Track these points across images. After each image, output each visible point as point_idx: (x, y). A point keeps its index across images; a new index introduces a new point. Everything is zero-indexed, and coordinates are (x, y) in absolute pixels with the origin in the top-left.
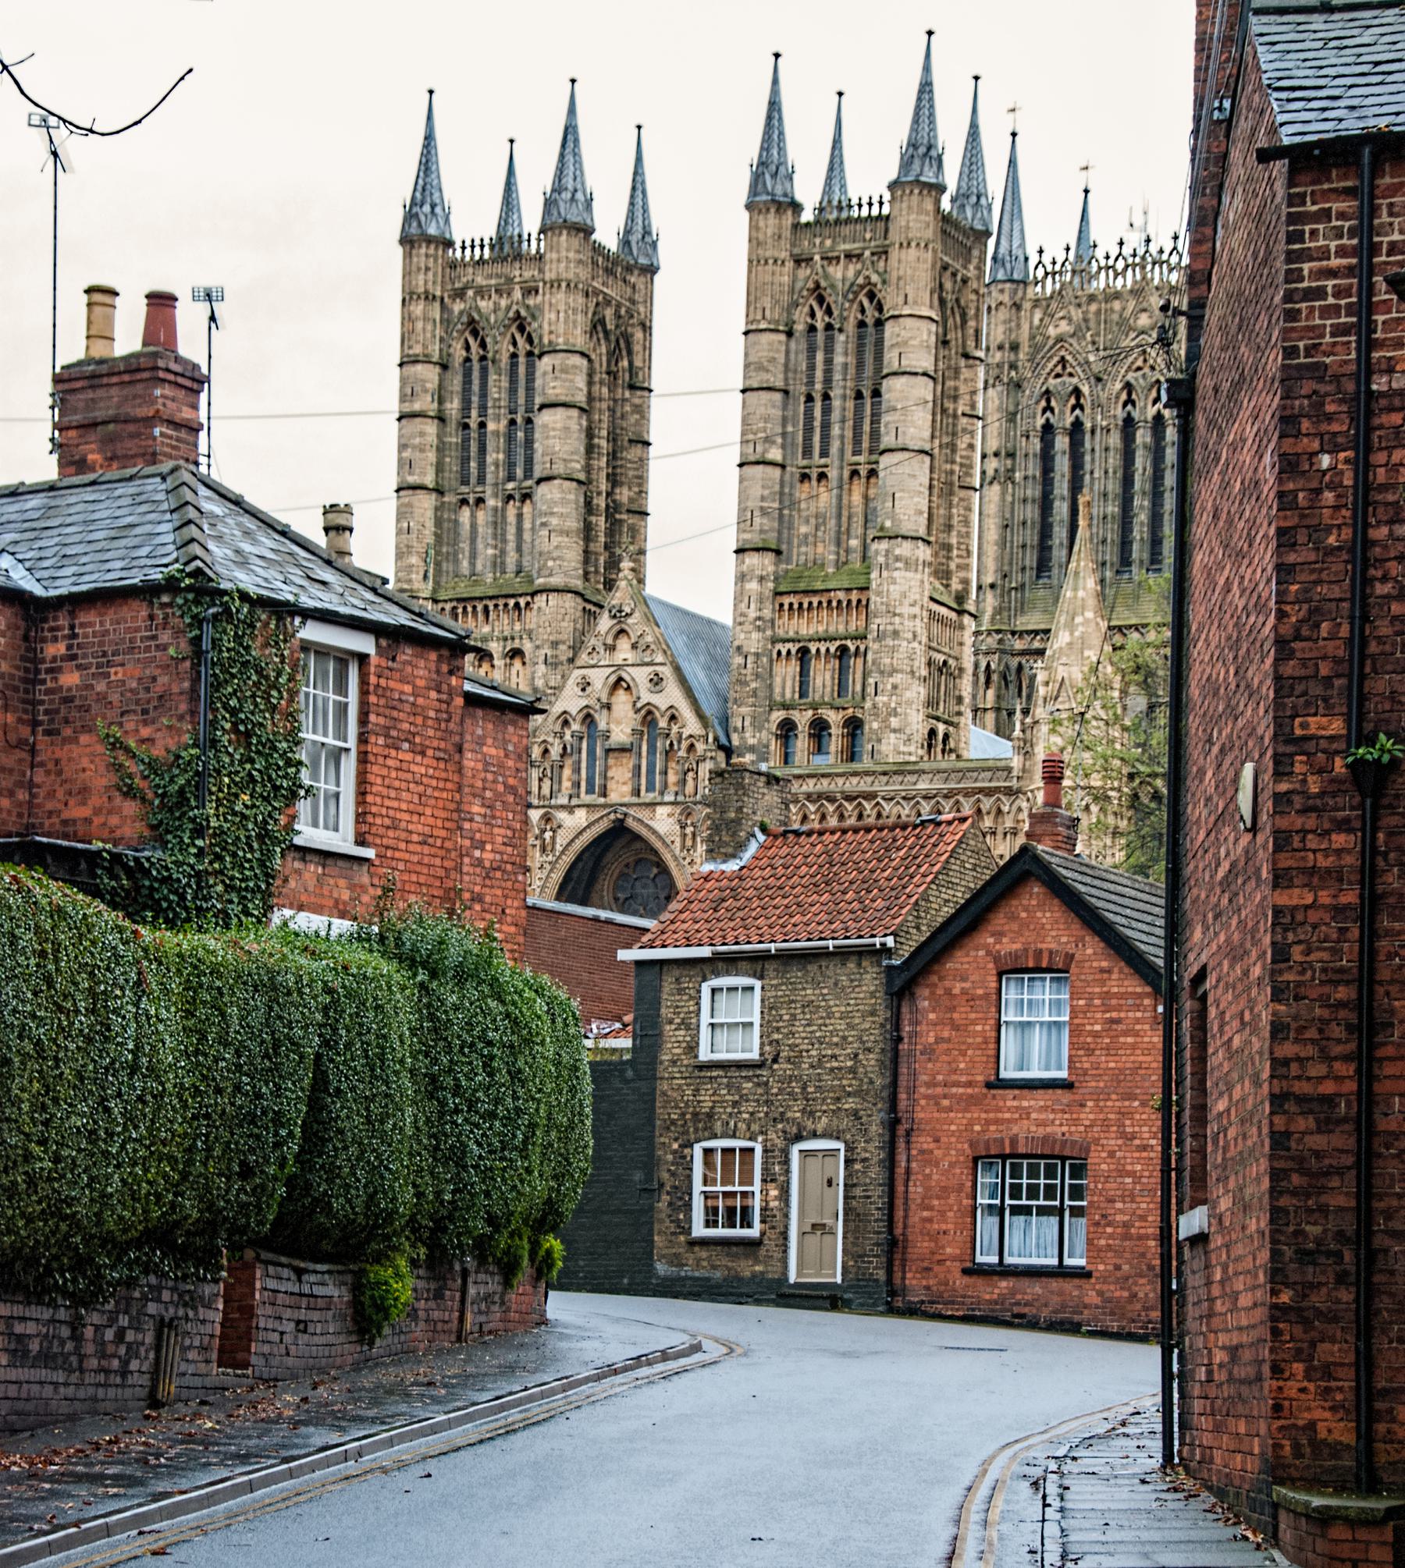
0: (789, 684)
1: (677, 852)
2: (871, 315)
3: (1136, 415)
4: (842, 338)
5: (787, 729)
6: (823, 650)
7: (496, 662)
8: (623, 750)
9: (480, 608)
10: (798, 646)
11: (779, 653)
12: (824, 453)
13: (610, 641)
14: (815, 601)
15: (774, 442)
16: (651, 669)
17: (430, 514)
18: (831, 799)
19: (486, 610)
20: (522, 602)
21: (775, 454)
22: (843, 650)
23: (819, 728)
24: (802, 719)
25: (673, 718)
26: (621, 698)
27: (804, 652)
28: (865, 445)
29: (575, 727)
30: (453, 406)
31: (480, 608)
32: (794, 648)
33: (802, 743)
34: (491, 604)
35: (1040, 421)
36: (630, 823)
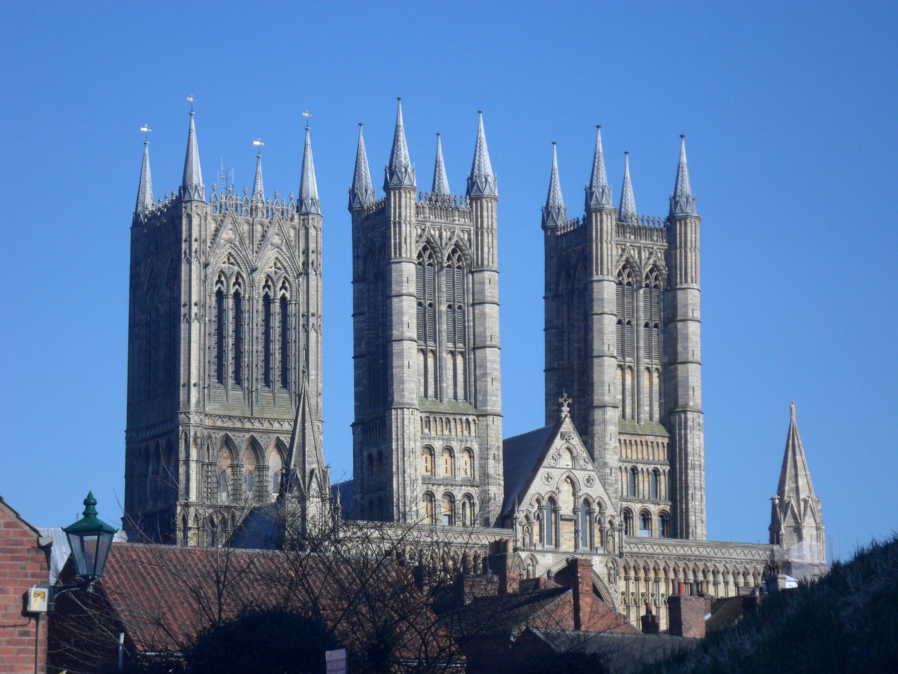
0: (625, 487)
1: (606, 584)
3: (271, 294)
5: (627, 514)
7: (456, 455)
14: (639, 439)
16: (587, 472)
18: (689, 560)
19: (448, 421)
20: (471, 418)
21: (615, 354)
22: (656, 472)
23: (646, 516)
24: (637, 507)
27: (634, 471)
29: (544, 503)
32: (629, 466)
33: (637, 522)
34: (451, 417)
35: (215, 289)
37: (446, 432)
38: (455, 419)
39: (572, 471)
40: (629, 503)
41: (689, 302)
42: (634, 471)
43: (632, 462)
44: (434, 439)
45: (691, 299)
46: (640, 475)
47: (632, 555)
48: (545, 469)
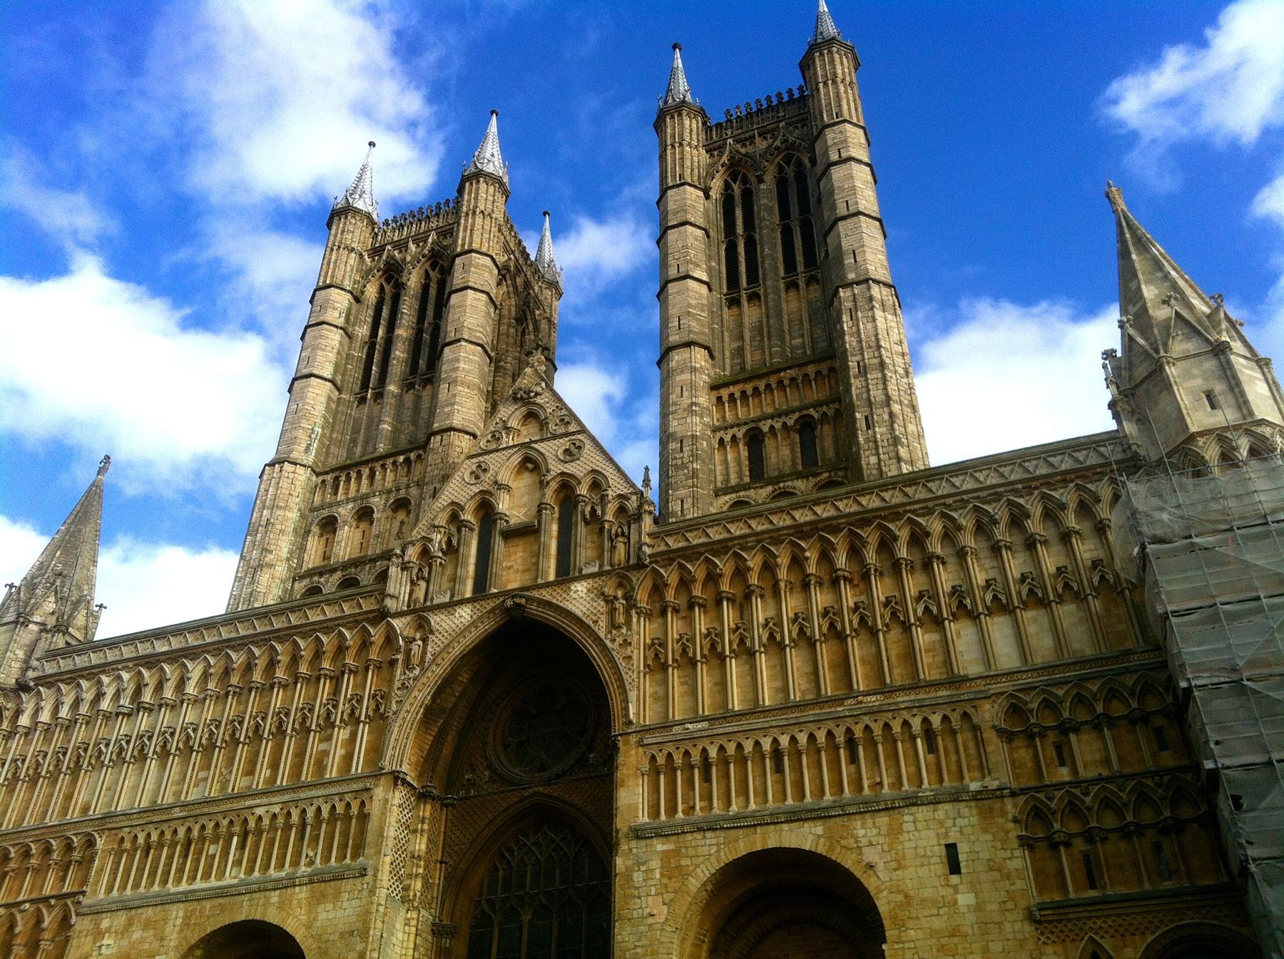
1: (602, 636)
2: (790, 171)
4: (762, 186)
6: (778, 426)
8: (528, 532)
9: (366, 472)
10: (744, 429)
11: (721, 441)
12: (753, 276)
13: (513, 423)
14: (762, 385)
15: (699, 266)
17: (323, 400)
18: (835, 530)
19: (372, 476)
20: (412, 456)
25: (595, 486)
26: (527, 480)
28: (800, 258)
29: (468, 516)
30: (363, 331)
31: (366, 472)
36: (534, 609)
37: (364, 488)
38: (383, 466)
39: (535, 446)
40: (742, 493)
41: (830, 142)
42: (755, 439)
43: (746, 424)
44: (339, 504)
45: (833, 139)
46: (769, 443)
47: (669, 557)
48: (475, 460)
